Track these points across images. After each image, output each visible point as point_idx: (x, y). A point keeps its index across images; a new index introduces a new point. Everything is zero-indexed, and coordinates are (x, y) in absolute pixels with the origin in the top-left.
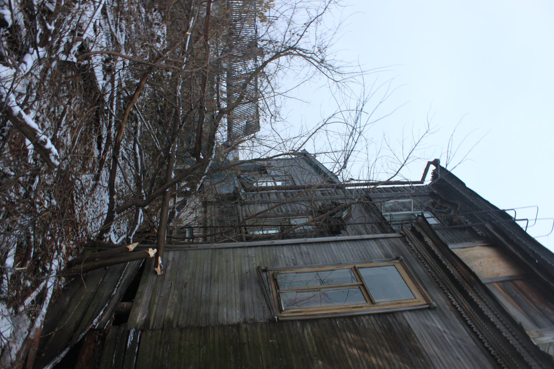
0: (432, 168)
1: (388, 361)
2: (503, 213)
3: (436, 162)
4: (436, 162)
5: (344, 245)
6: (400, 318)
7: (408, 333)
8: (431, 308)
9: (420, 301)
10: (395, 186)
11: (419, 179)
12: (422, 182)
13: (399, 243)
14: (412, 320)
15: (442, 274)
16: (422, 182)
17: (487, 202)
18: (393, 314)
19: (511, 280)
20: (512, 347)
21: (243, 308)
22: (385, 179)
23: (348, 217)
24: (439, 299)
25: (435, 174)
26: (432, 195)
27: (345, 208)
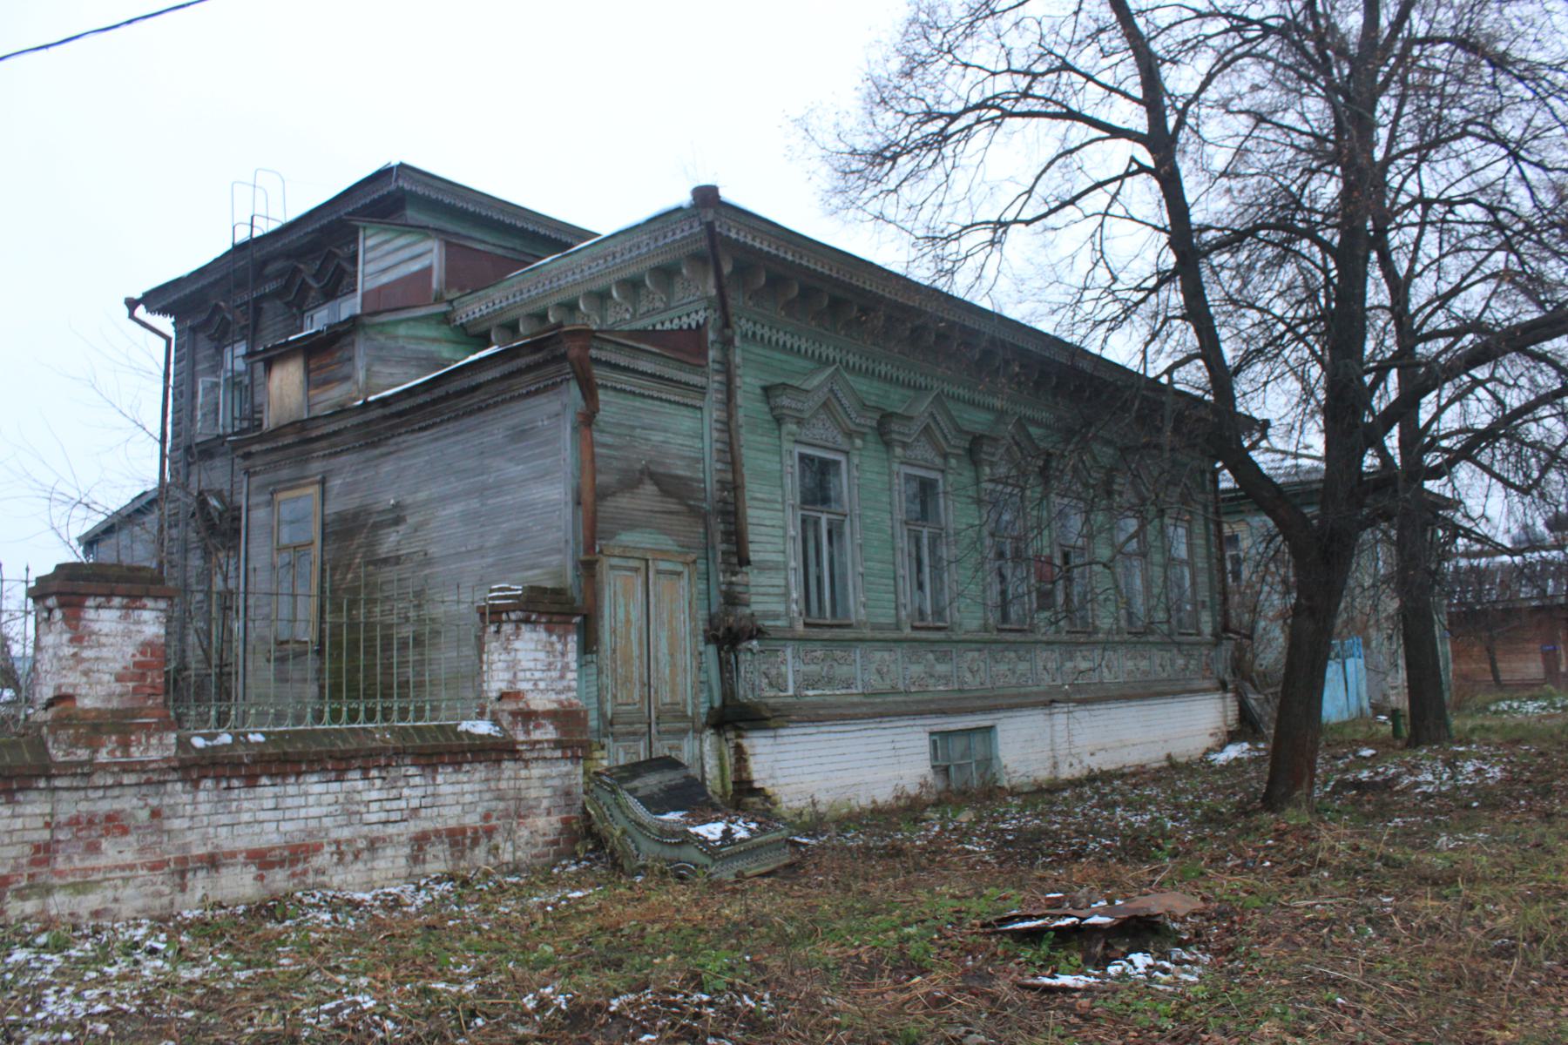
0: (141, 312)
1: (359, 547)
2: (238, 249)
3: (132, 304)
4: (132, 304)
5: (251, 551)
6: (328, 520)
7: (342, 517)
8: (323, 482)
9: (314, 490)
10: (171, 382)
11: (163, 342)
12: (168, 340)
13: (256, 481)
14: (333, 507)
15: (293, 451)
16: (168, 340)
17: (216, 260)
18: (324, 525)
19: (308, 371)
20: (358, 425)
21: (305, 680)
22: (158, 447)
23: (219, 495)
24: (316, 467)
25: (150, 310)
26: (194, 330)
27: (203, 503)
